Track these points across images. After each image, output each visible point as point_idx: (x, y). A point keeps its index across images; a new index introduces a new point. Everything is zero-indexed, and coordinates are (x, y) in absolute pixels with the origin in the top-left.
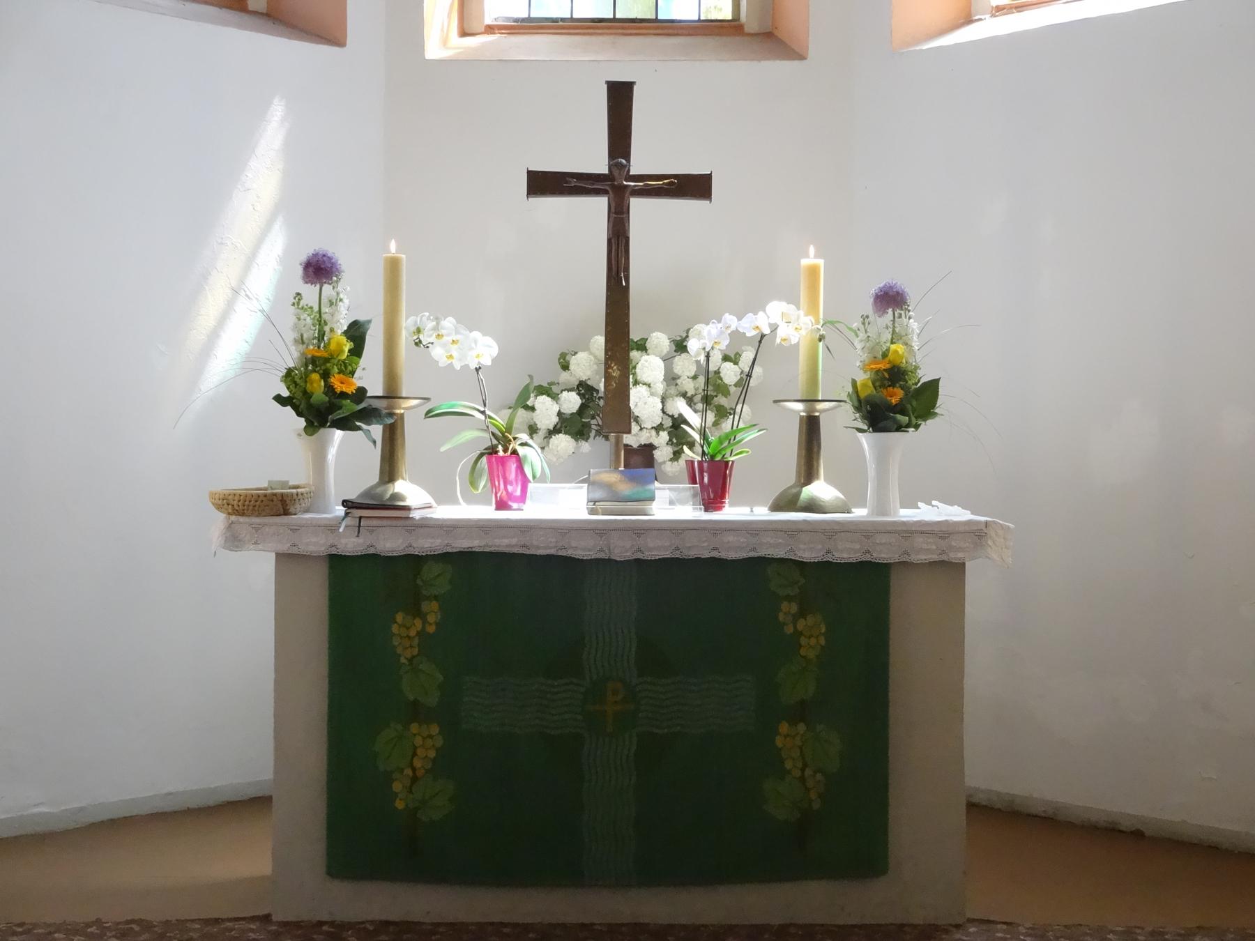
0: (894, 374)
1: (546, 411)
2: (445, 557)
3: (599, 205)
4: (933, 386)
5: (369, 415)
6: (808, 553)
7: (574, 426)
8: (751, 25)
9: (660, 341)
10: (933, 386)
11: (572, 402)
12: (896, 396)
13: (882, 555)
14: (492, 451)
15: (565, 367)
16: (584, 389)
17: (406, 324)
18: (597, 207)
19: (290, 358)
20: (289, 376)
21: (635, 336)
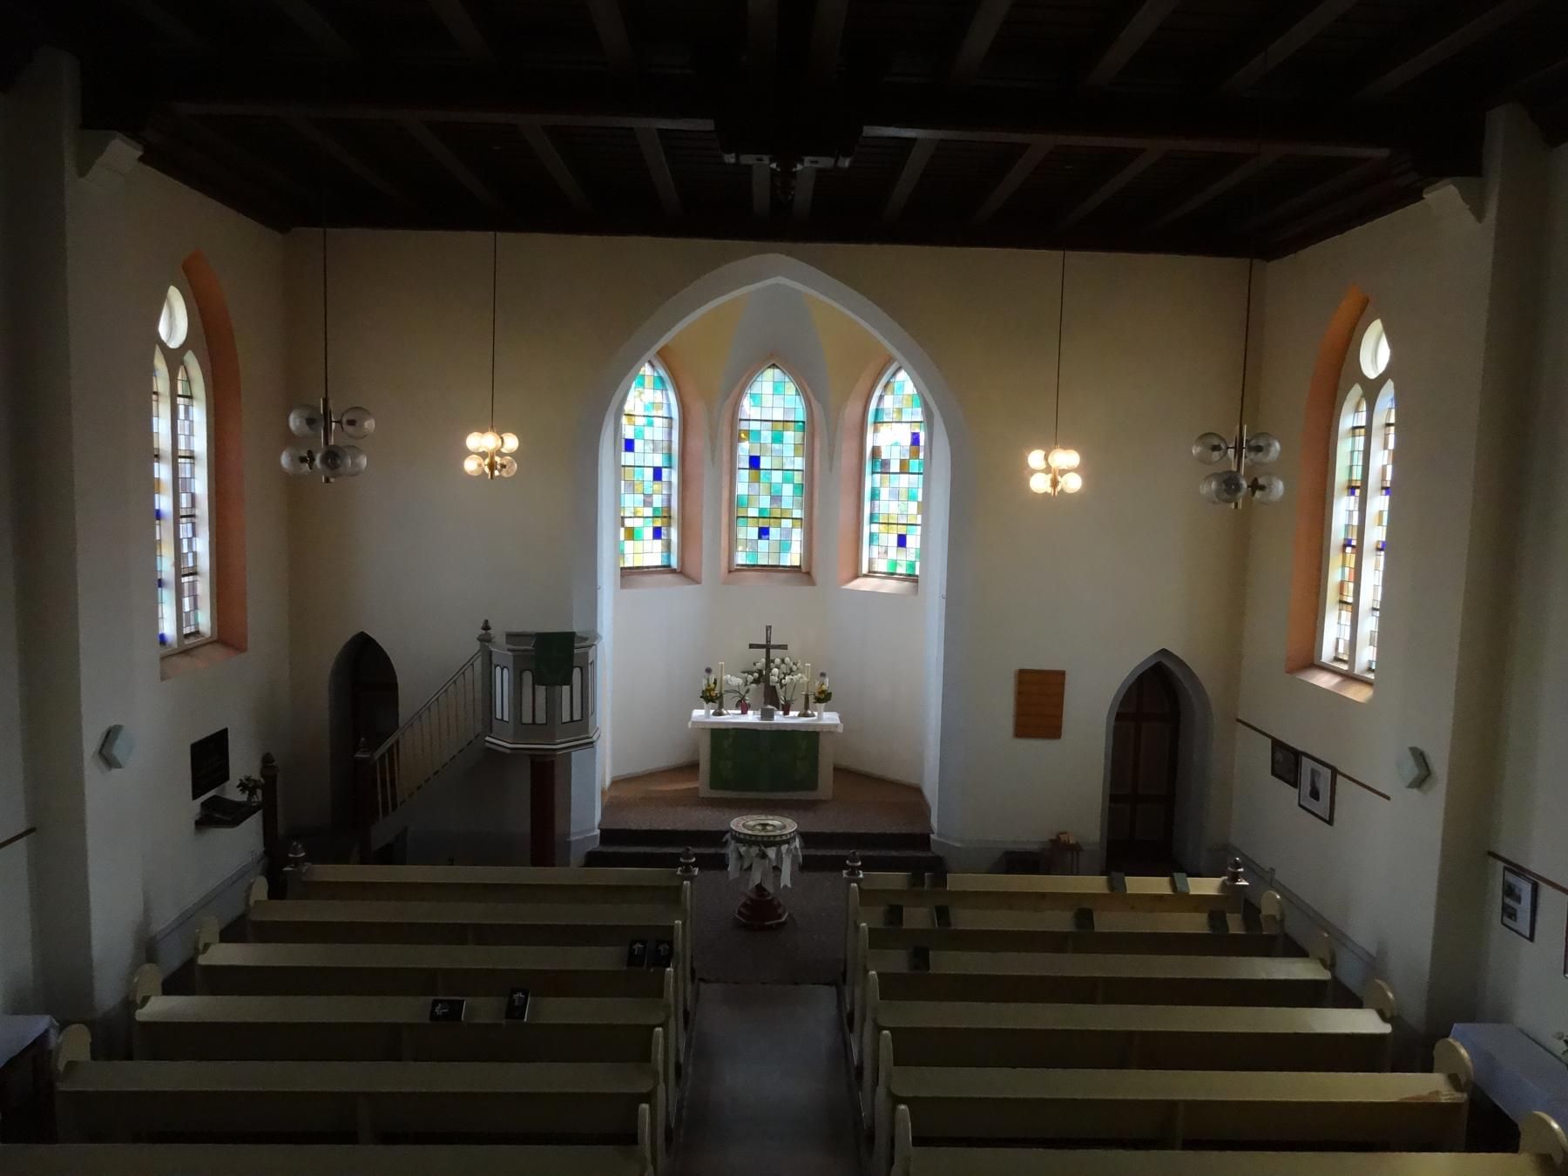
0: (822, 692)
1: (750, 678)
2: (734, 729)
3: (764, 650)
4: (831, 693)
5: (717, 698)
6: (803, 729)
7: (756, 681)
8: (804, 569)
9: (778, 661)
10: (831, 693)
11: (756, 675)
12: (823, 696)
13: (818, 730)
14: (740, 701)
15: (755, 664)
16: (760, 672)
17: (724, 677)
18: (764, 650)
19: (704, 689)
20: (703, 691)
21: (771, 658)
